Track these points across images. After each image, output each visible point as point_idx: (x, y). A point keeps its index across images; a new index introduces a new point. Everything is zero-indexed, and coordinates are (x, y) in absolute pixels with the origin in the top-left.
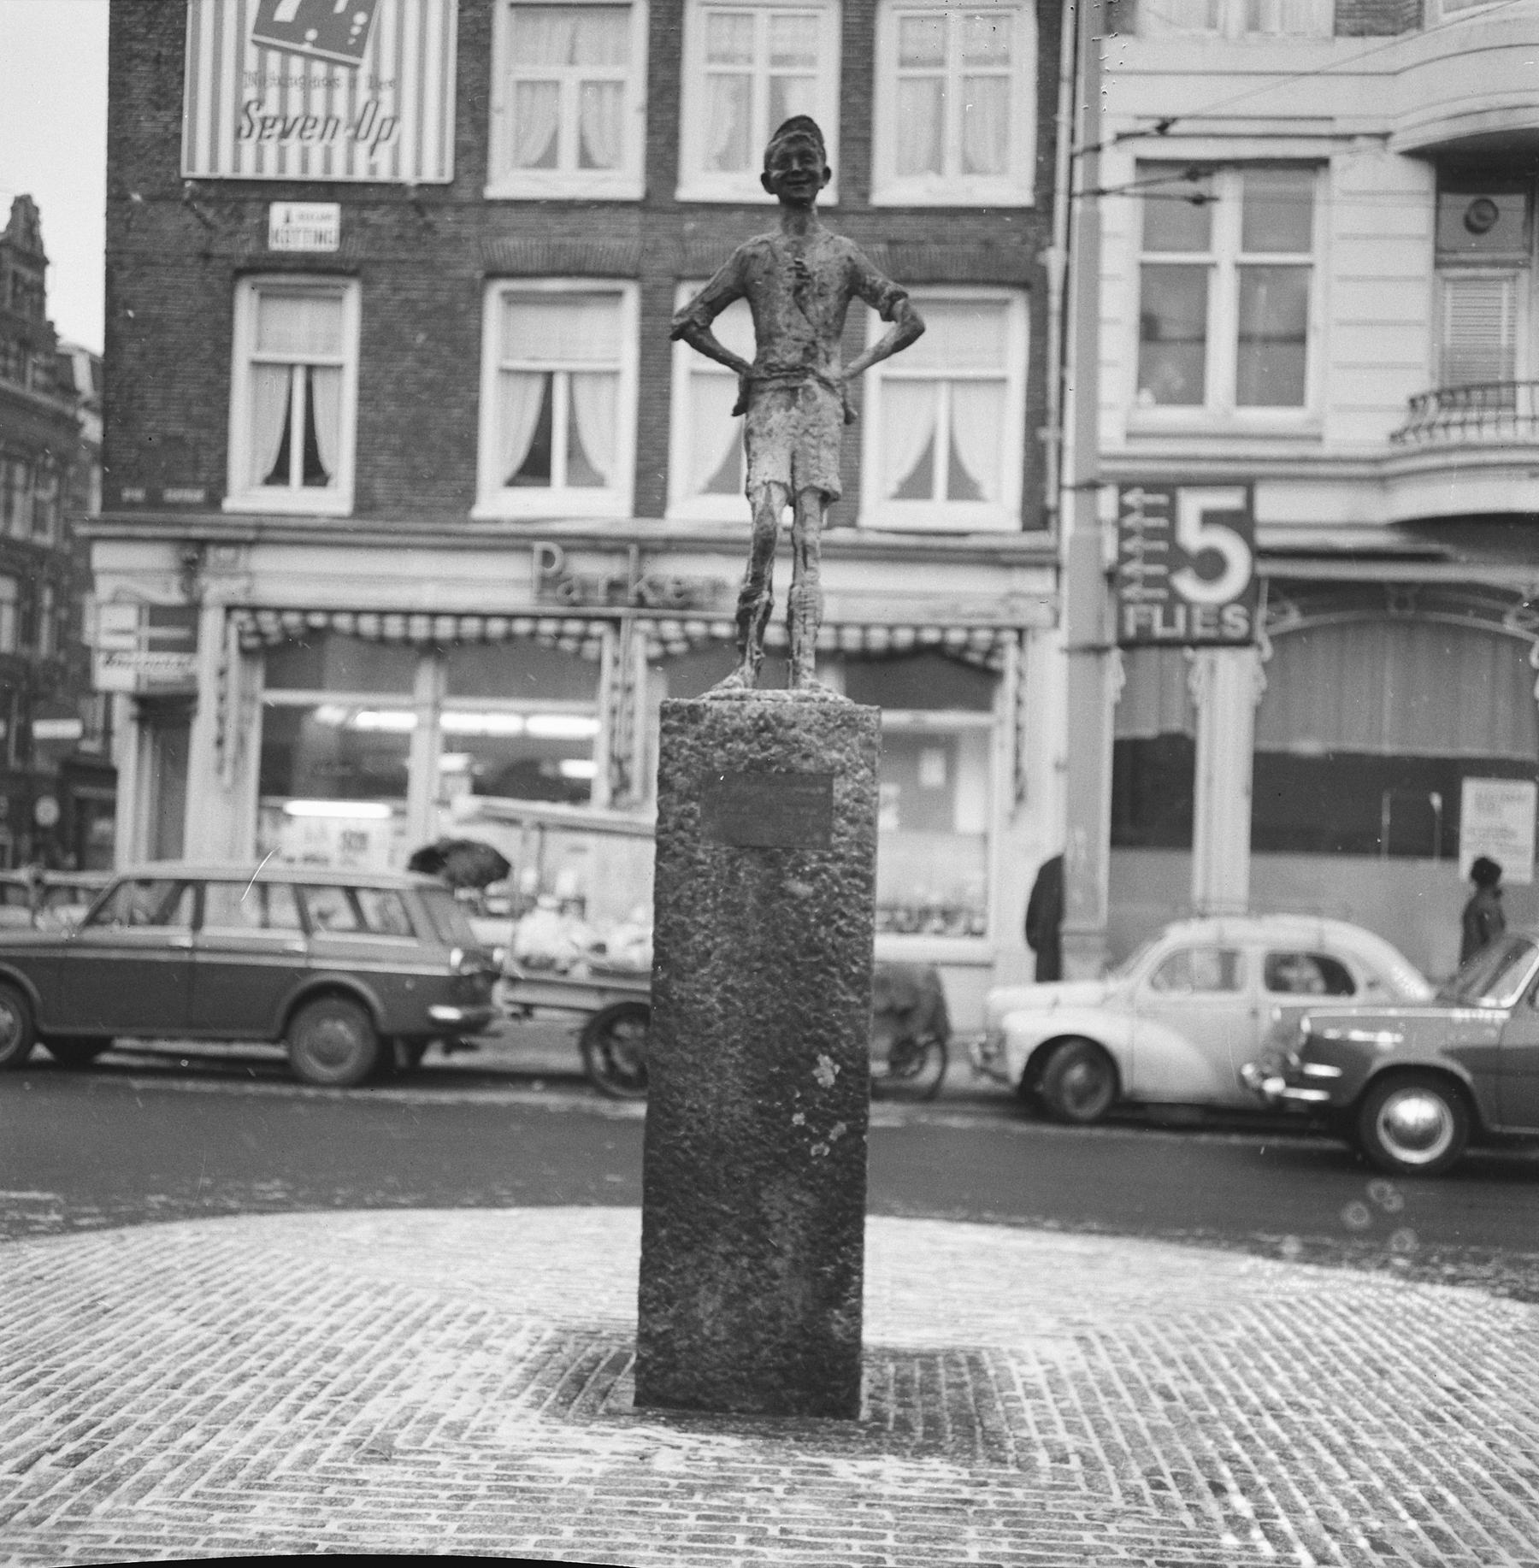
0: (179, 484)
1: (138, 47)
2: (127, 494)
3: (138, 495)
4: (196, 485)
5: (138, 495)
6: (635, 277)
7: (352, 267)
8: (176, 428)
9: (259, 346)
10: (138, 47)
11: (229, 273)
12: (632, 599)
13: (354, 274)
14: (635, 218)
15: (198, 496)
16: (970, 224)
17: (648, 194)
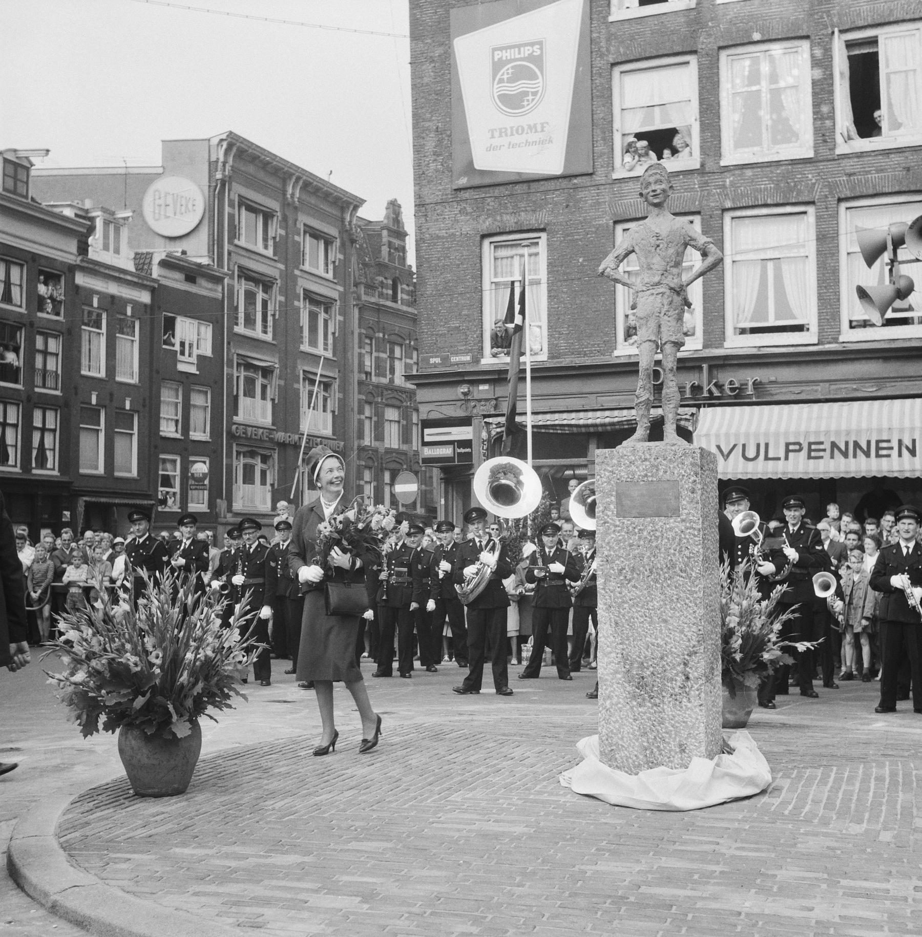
0: (456, 353)
1: (427, 124)
2: (432, 361)
3: (438, 360)
4: (466, 352)
5: (438, 360)
6: (698, 213)
7: (542, 226)
8: (455, 324)
9: (496, 276)
10: (427, 124)
11: (478, 238)
12: (706, 394)
13: (543, 230)
14: (696, 180)
15: (468, 358)
16: (895, 158)
17: (702, 165)
